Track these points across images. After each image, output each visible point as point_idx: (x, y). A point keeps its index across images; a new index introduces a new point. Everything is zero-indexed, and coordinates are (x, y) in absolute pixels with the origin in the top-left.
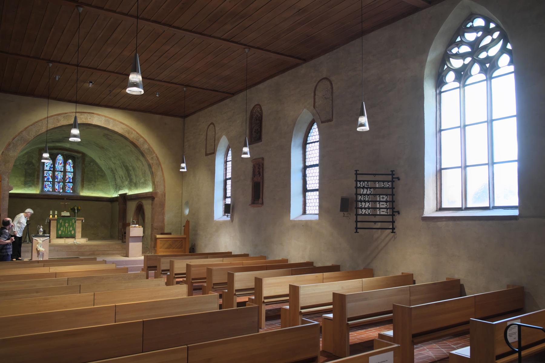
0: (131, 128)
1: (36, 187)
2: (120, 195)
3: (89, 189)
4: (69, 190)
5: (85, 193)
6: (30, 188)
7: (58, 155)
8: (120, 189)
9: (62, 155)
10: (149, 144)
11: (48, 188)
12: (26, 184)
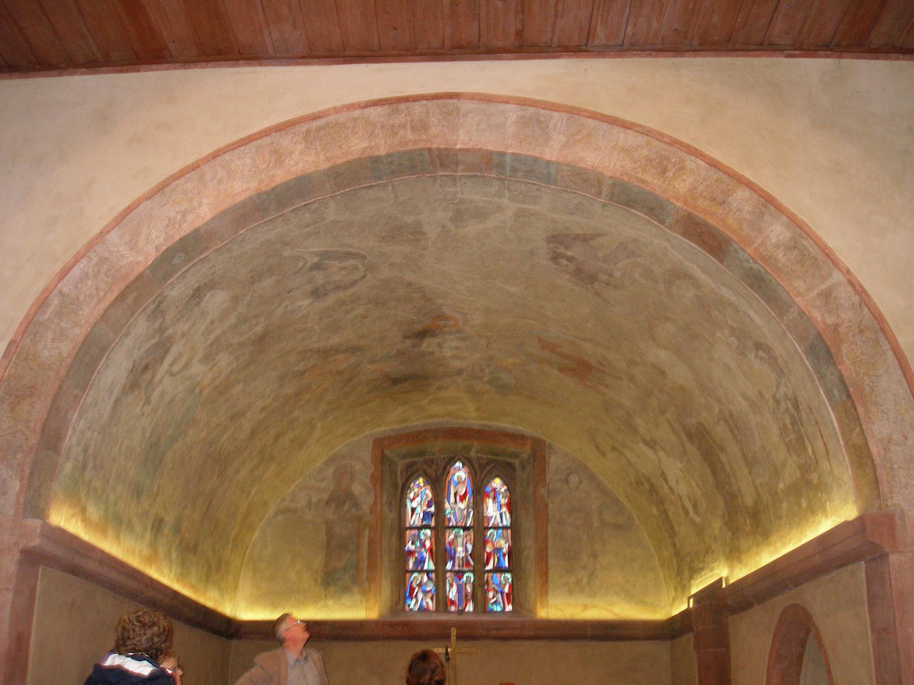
0: (674, 143)
1: (365, 592)
2: (699, 597)
4: (499, 606)
5: (557, 608)
6: (346, 600)
7: (451, 461)
8: (695, 571)
10: (793, 220)
11: (421, 601)
12: (331, 581)
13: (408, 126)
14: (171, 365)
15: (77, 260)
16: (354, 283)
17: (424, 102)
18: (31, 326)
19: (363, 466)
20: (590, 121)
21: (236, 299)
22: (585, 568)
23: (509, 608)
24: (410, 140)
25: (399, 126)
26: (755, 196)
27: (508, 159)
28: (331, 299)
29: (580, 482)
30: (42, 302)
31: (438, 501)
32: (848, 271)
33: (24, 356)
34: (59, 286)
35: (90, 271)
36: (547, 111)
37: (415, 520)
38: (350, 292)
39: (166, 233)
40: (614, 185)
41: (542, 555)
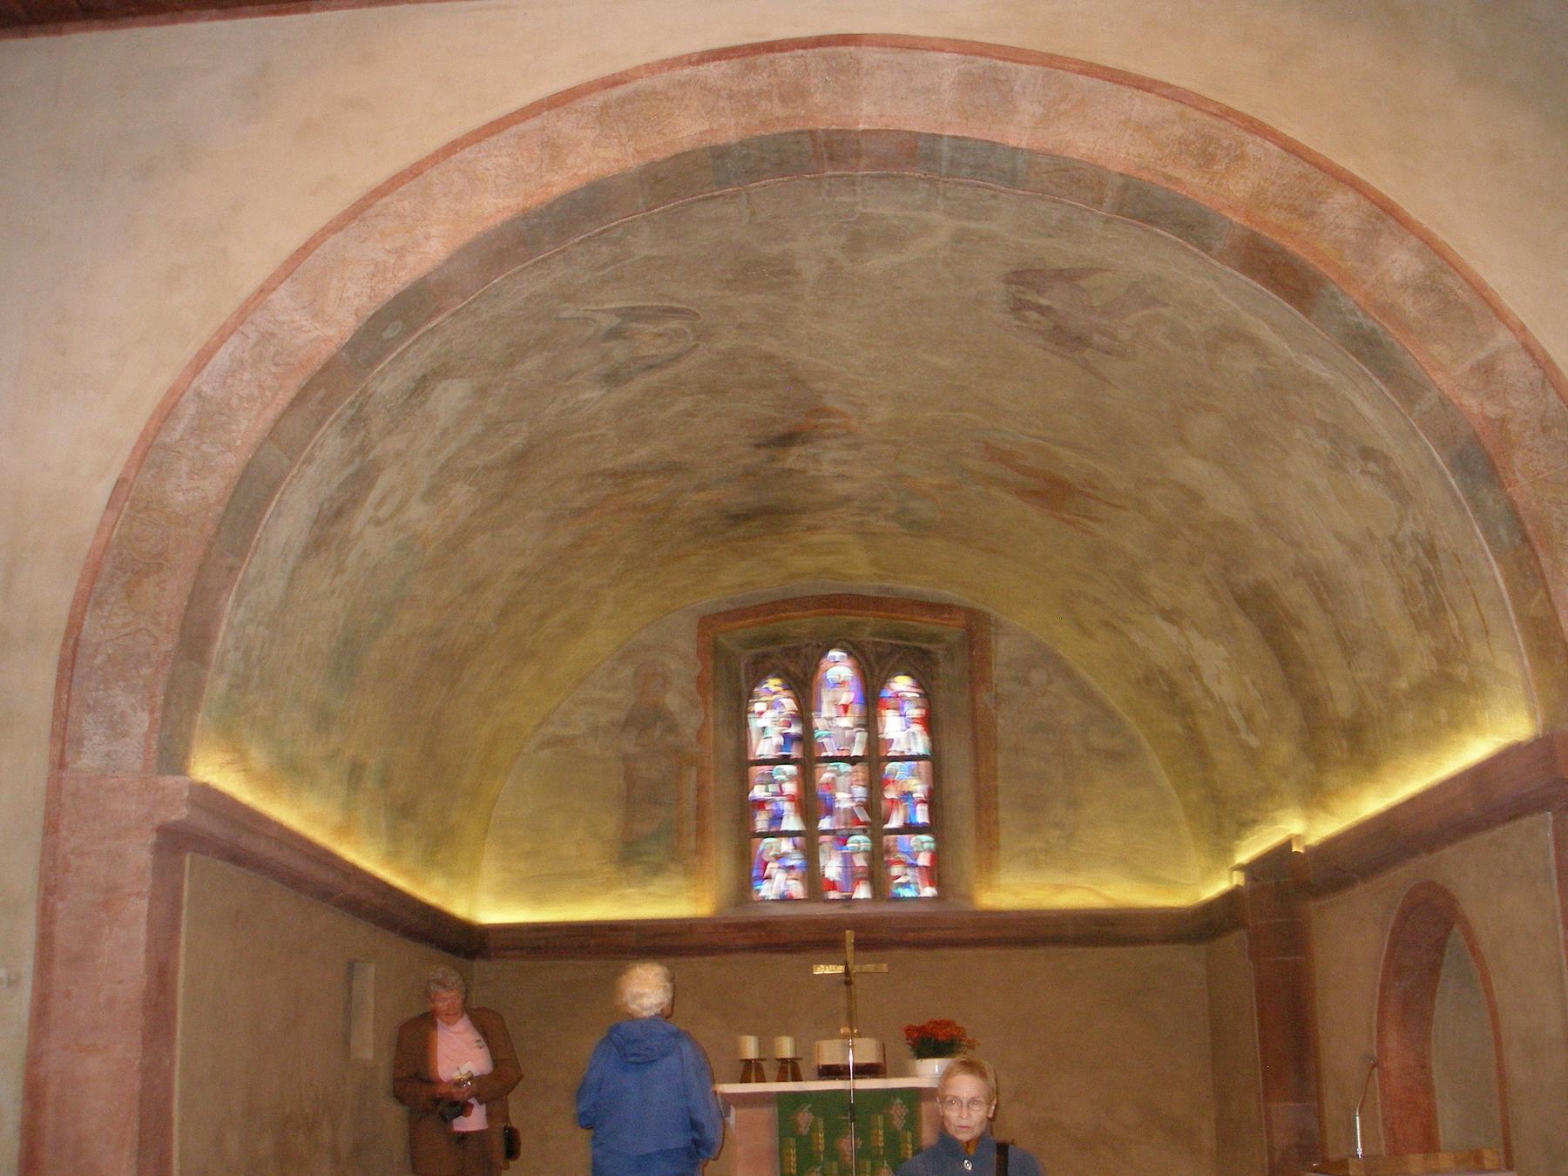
0: (1226, 113)
1: (689, 872)
3: (1038, 860)
4: (912, 887)
5: (1012, 890)
6: (658, 886)
8: (1244, 825)
9: (855, 652)
10: (1429, 244)
12: (634, 855)
13: (775, 92)
14: (377, 507)
15: (222, 336)
16: (676, 358)
17: (800, 52)
18: (150, 451)
19: (681, 663)
20: (1083, 79)
21: (482, 392)
22: (1057, 825)
23: (929, 892)
24: (777, 116)
25: (759, 94)
26: (1365, 203)
27: (945, 148)
28: (636, 387)
29: (1050, 682)
30: (167, 412)
31: (805, 713)
32: (1523, 328)
33: (143, 504)
34: (195, 383)
35: (246, 356)
36: (1009, 64)
37: (765, 747)
38: (668, 373)
39: (373, 289)
40: (1126, 187)
41: (985, 804)
